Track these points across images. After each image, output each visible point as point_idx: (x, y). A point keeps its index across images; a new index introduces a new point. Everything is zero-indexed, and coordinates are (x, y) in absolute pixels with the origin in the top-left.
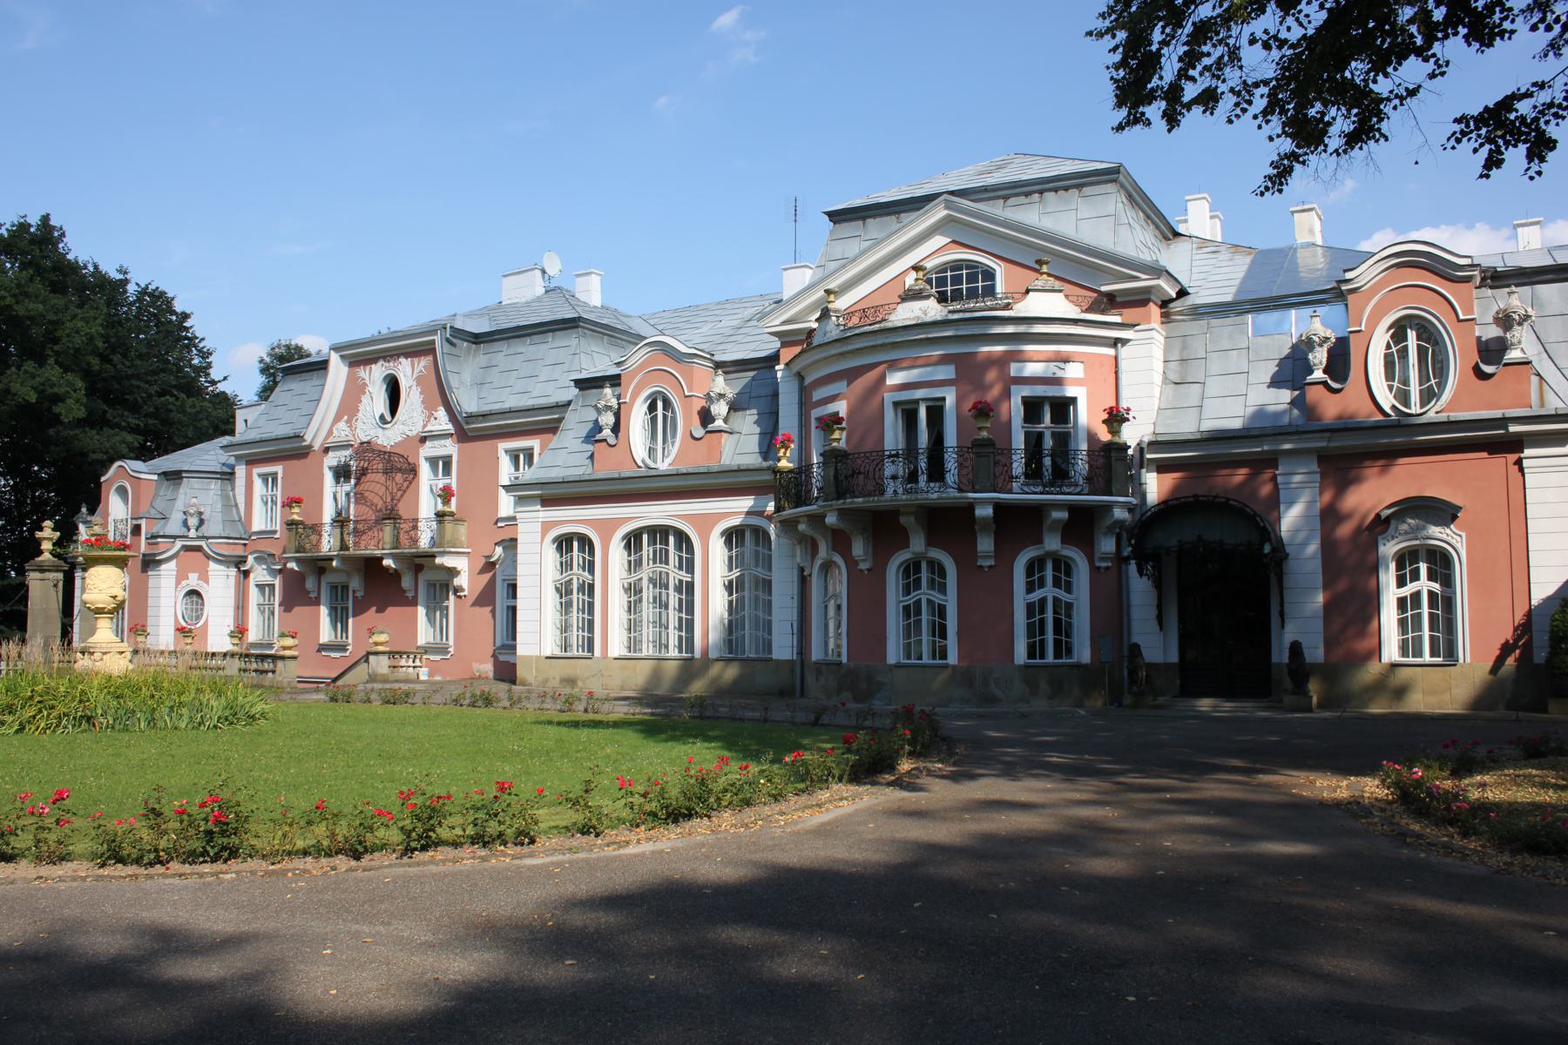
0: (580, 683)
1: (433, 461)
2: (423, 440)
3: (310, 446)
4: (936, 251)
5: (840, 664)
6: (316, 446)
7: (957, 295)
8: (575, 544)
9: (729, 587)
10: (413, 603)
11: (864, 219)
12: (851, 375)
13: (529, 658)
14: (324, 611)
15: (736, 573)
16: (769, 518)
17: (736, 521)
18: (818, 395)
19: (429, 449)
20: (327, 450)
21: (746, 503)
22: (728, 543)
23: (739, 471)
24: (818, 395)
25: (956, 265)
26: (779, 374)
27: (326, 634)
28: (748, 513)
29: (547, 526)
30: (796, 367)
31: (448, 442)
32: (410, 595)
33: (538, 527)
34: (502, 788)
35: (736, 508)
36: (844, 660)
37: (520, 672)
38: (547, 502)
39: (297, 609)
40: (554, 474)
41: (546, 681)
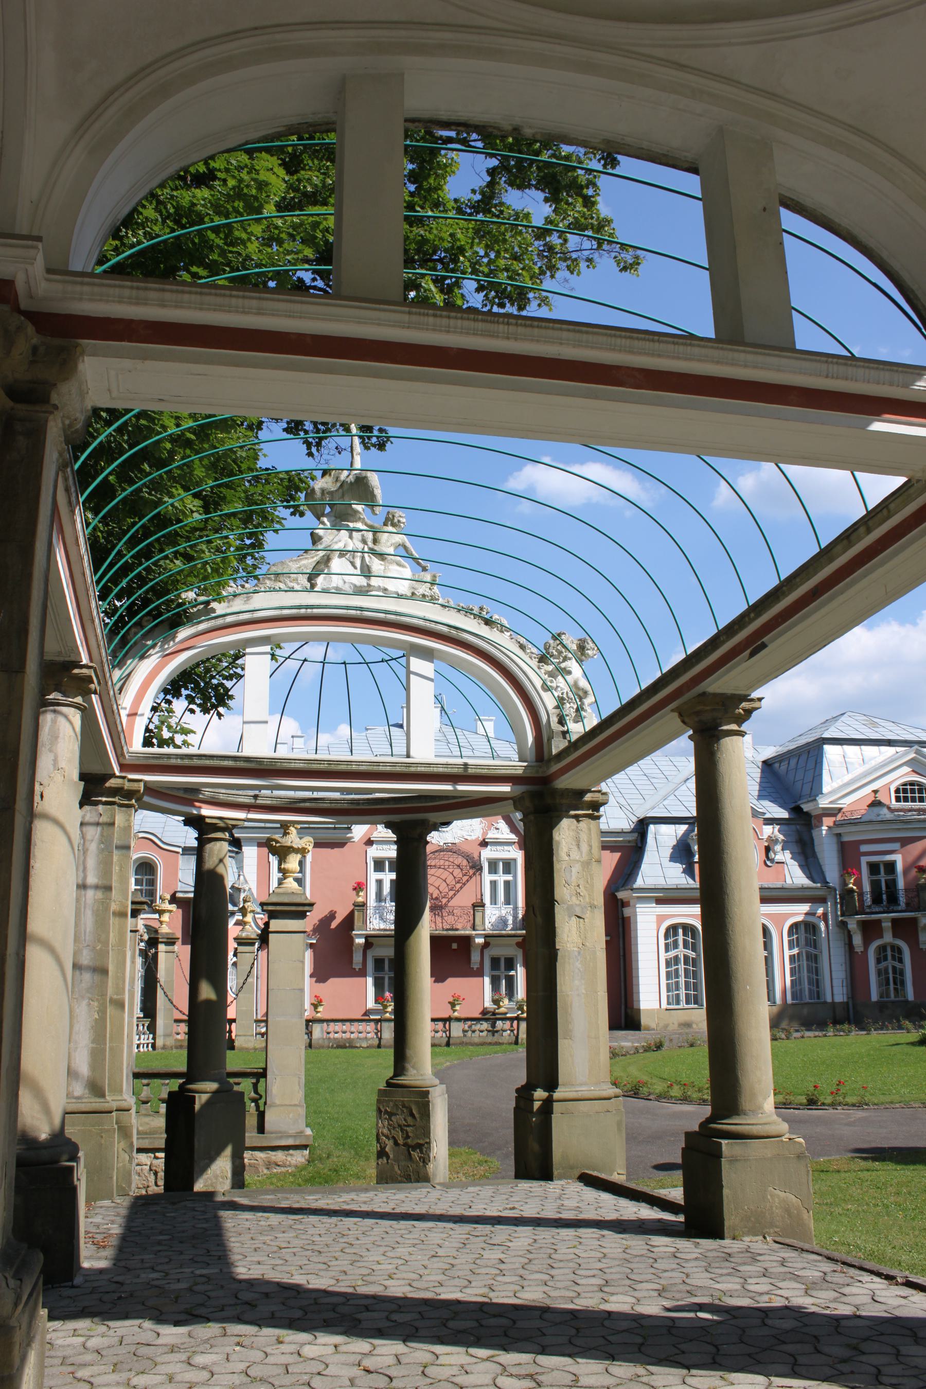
0: (694, 1026)
1: (493, 865)
2: (484, 844)
3: (352, 838)
4: (904, 775)
5: (907, 1002)
6: (356, 839)
7: (906, 800)
8: (680, 931)
9: (792, 958)
10: (480, 973)
11: (841, 744)
12: (905, 842)
13: (650, 1012)
14: (370, 981)
15: (795, 951)
16: (819, 917)
17: (800, 918)
18: (864, 848)
19: (487, 854)
20: (370, 842)
21: (805, 908)
22: (790, 933)
23: (803, 888)
24: (864, 848)
25: (912, 784)
26: (824, 832)
27: (371, 1004)
28: (806, 914)
29: (661, 919)
30: (839, 830)
31: (510, 848)
32: (475, 965)
33: (654, 919)
34: (816, 1087)
35: (798, 911)
36: (911, 996)
37: (644, 1021)
38: (660, 901)
39: (332, 981)
40: (660, 882)
41: (666, 1026)
